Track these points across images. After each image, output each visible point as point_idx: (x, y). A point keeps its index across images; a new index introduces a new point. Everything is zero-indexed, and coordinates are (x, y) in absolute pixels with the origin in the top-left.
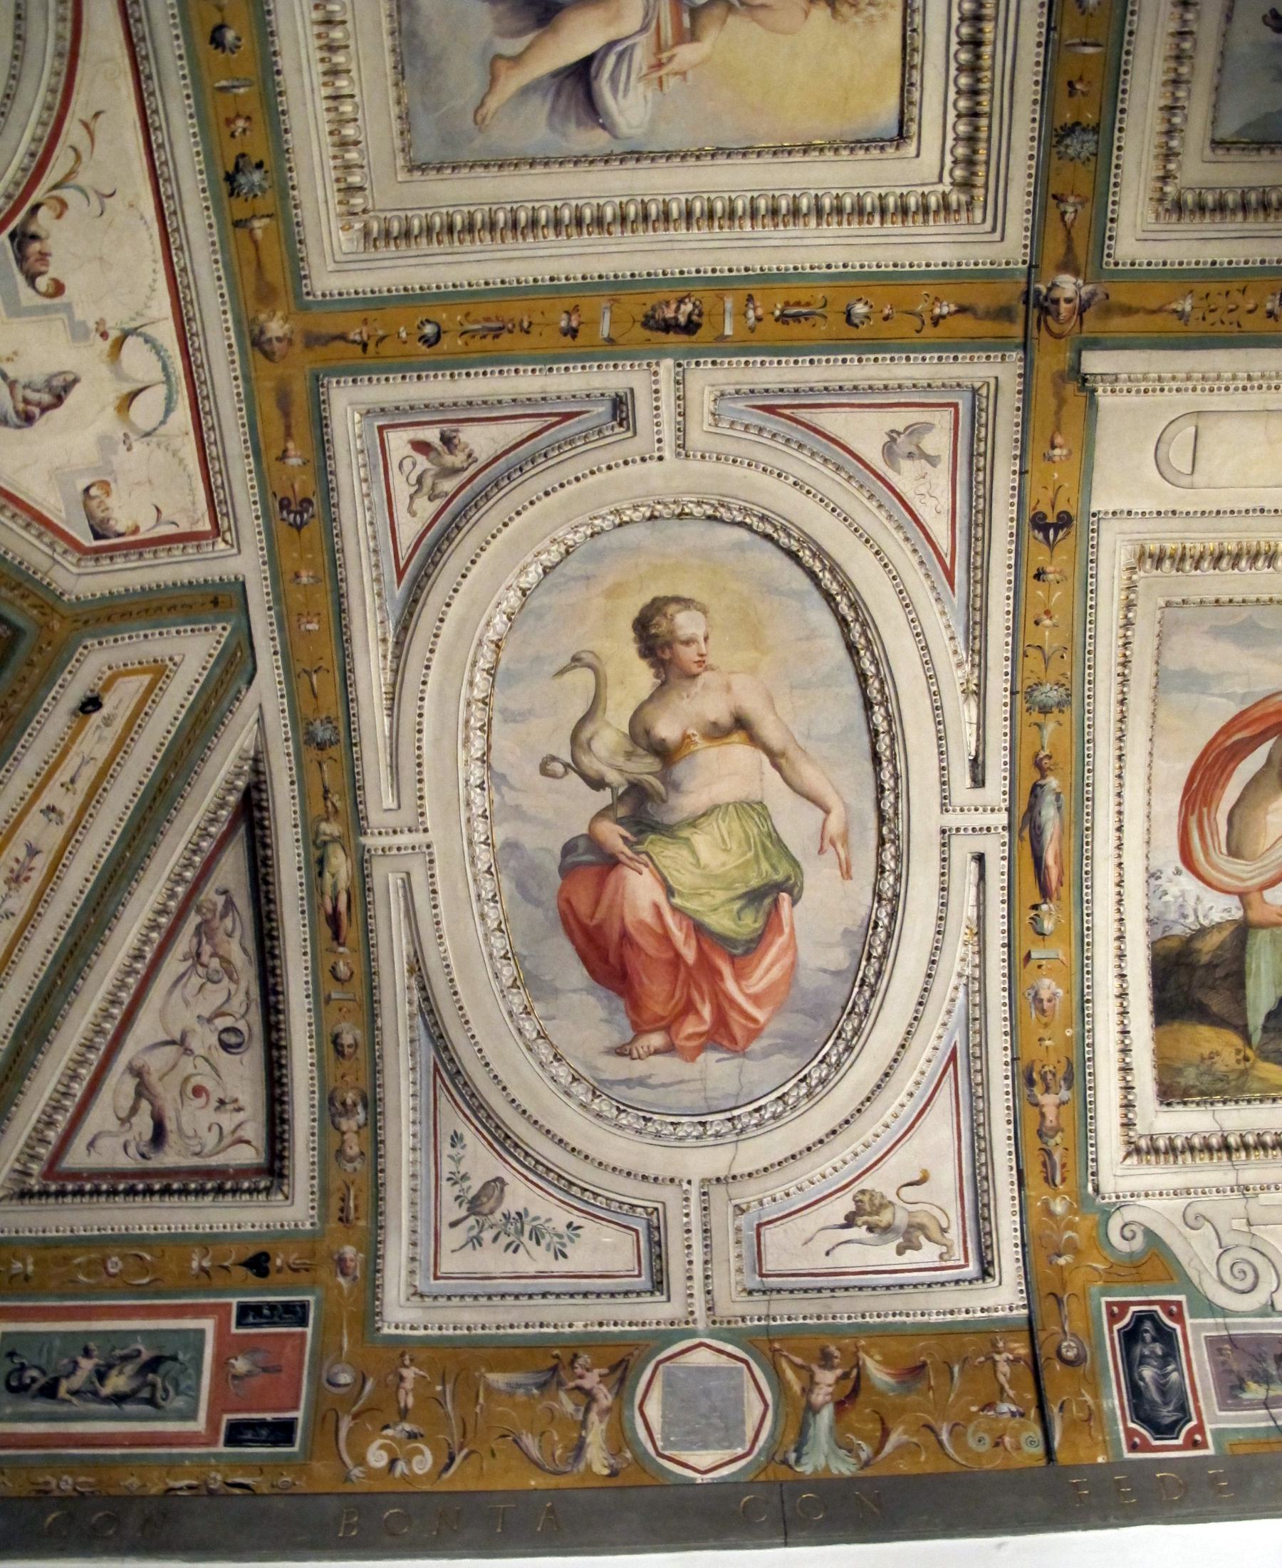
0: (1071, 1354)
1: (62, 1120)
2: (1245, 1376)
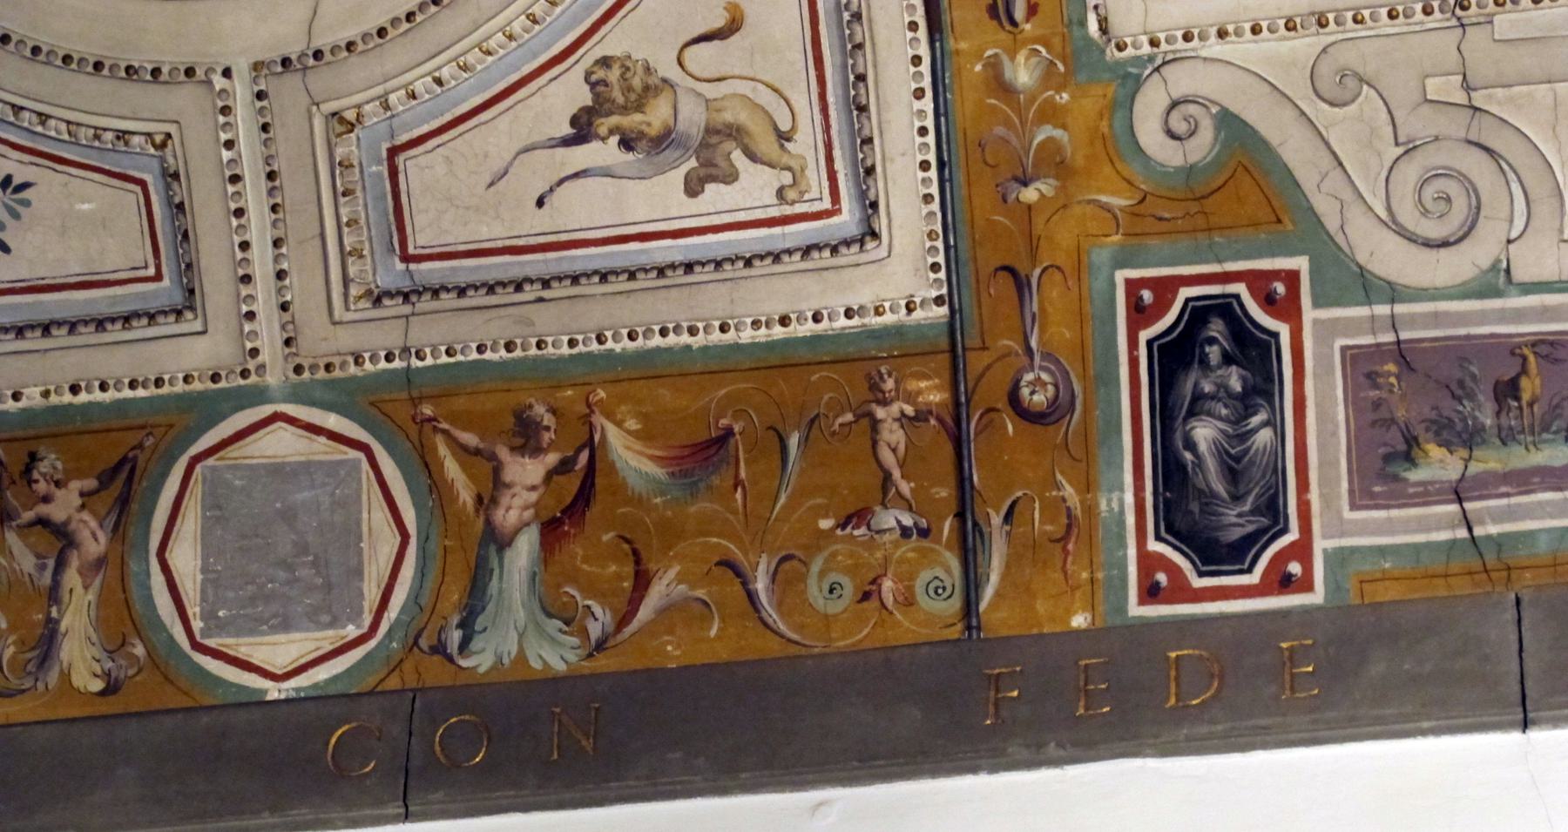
0: (1040, 399)
2: (1419, 431)
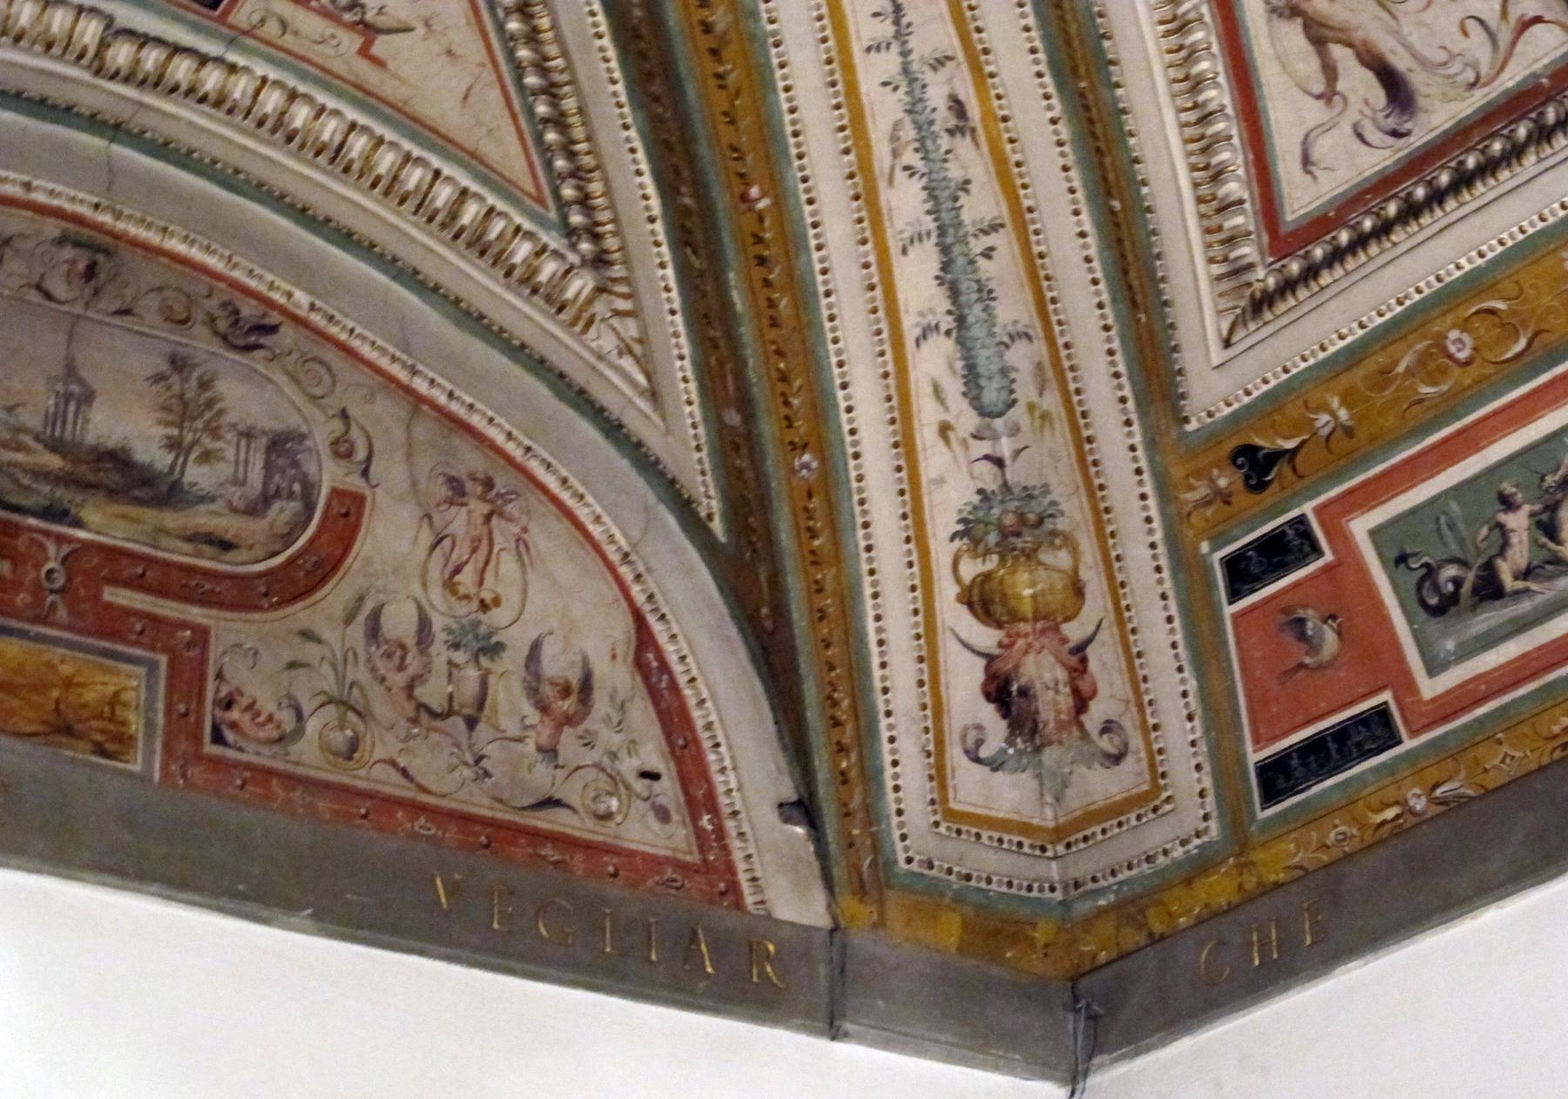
1: (1232, 156)
